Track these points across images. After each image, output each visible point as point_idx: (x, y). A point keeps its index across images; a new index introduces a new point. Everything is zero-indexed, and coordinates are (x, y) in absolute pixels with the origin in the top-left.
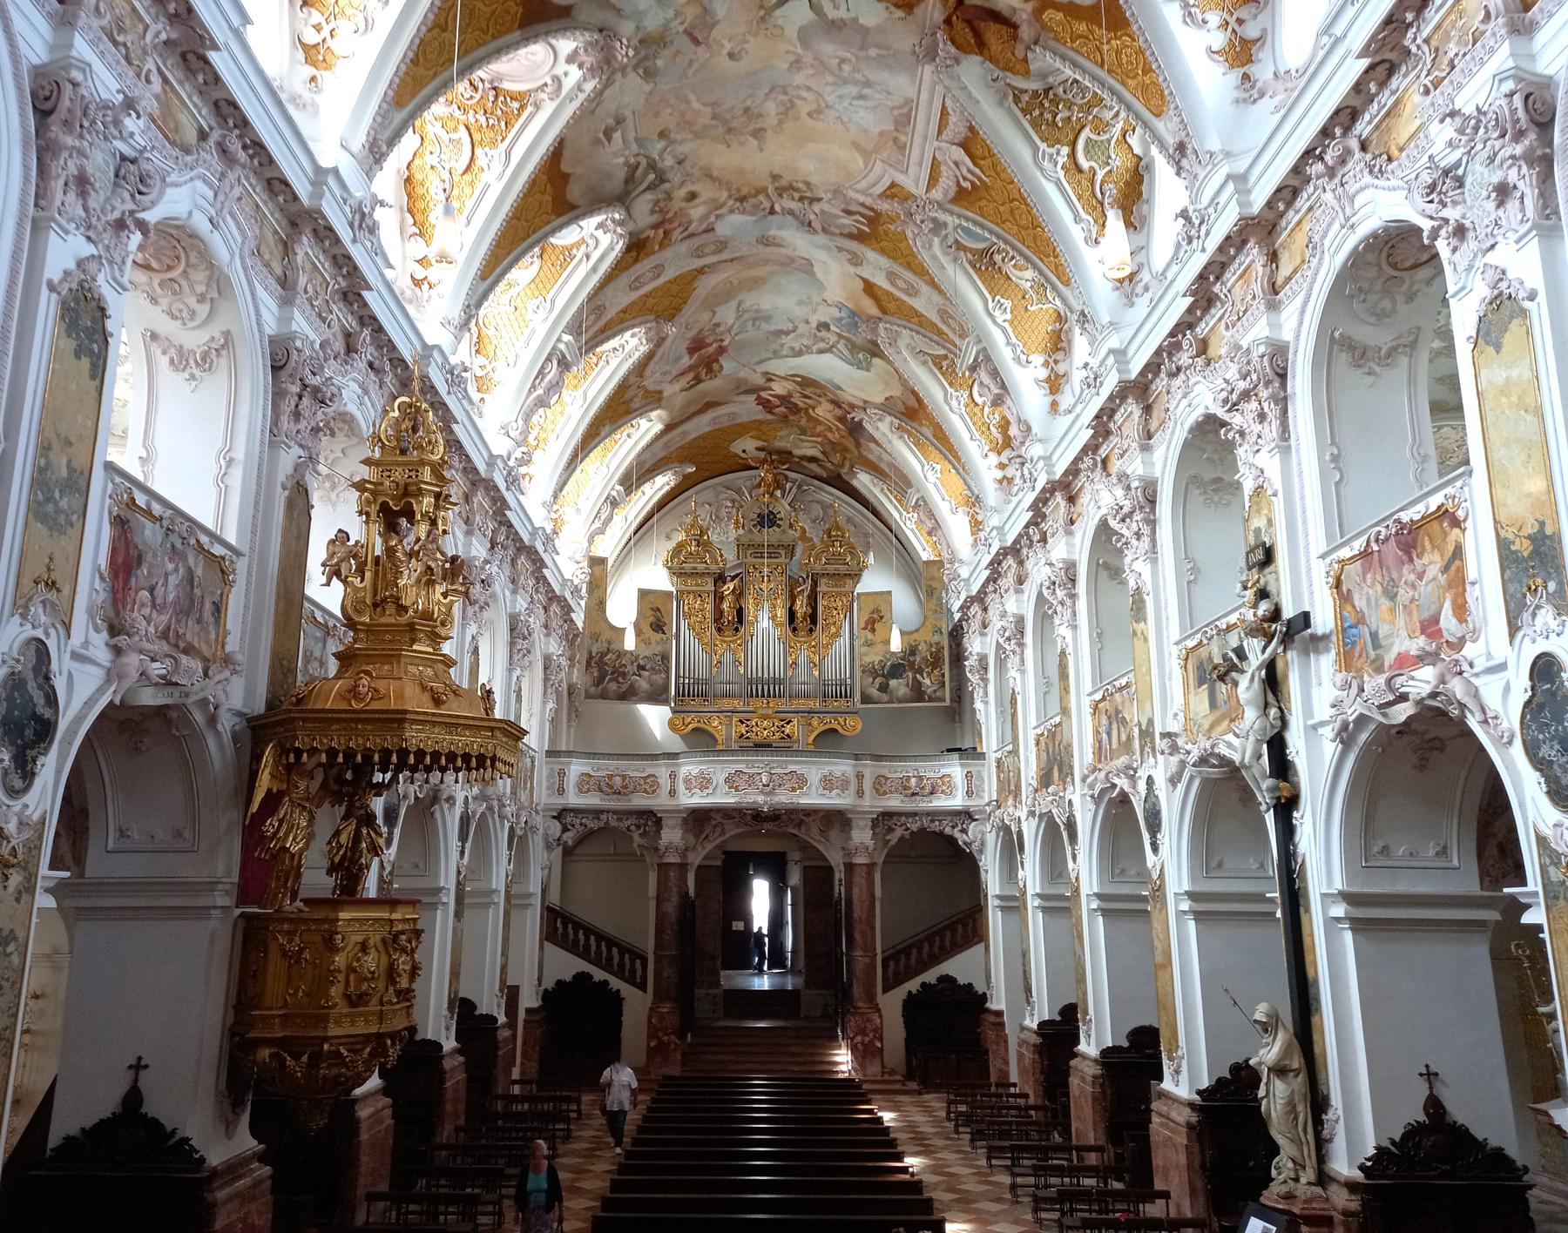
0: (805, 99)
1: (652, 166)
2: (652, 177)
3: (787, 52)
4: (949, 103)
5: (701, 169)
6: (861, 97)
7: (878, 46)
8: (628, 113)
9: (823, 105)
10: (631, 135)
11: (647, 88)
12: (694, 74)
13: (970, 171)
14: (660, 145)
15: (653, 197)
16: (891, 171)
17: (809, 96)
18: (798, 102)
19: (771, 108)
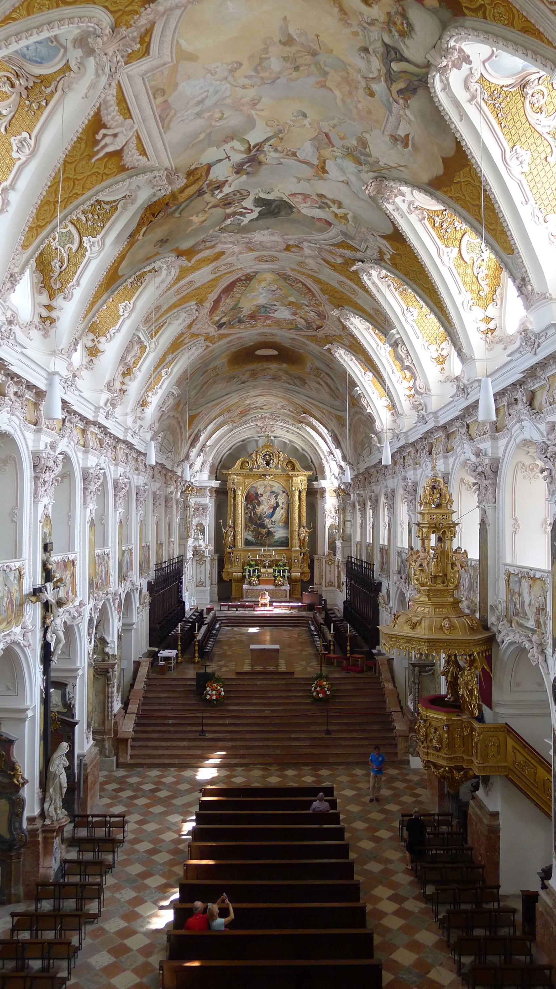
0: (246, 77)
1: (390, 78)
2: (395, 66)
3: (263, 110)
4: (145, 159)
5: (349, 25)
6: (201, 102)
7: (200, 142)
8: (387, 138)
9: (230, 79)
10: (392, 119)
11: (367, 136)
12: (333, 119)
13: (106, 145)
14: (375, 87)
15: (402, 45)
16: (155, 63)
17: (243, 81)
18: (252, 73)
19: (275, 64)
